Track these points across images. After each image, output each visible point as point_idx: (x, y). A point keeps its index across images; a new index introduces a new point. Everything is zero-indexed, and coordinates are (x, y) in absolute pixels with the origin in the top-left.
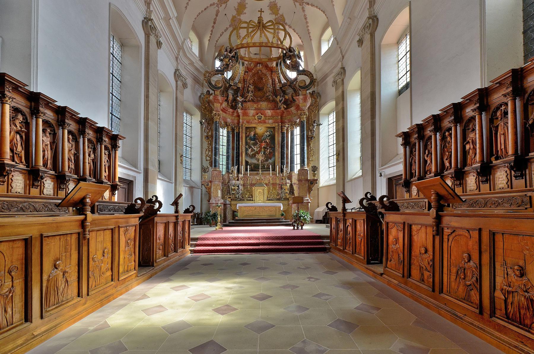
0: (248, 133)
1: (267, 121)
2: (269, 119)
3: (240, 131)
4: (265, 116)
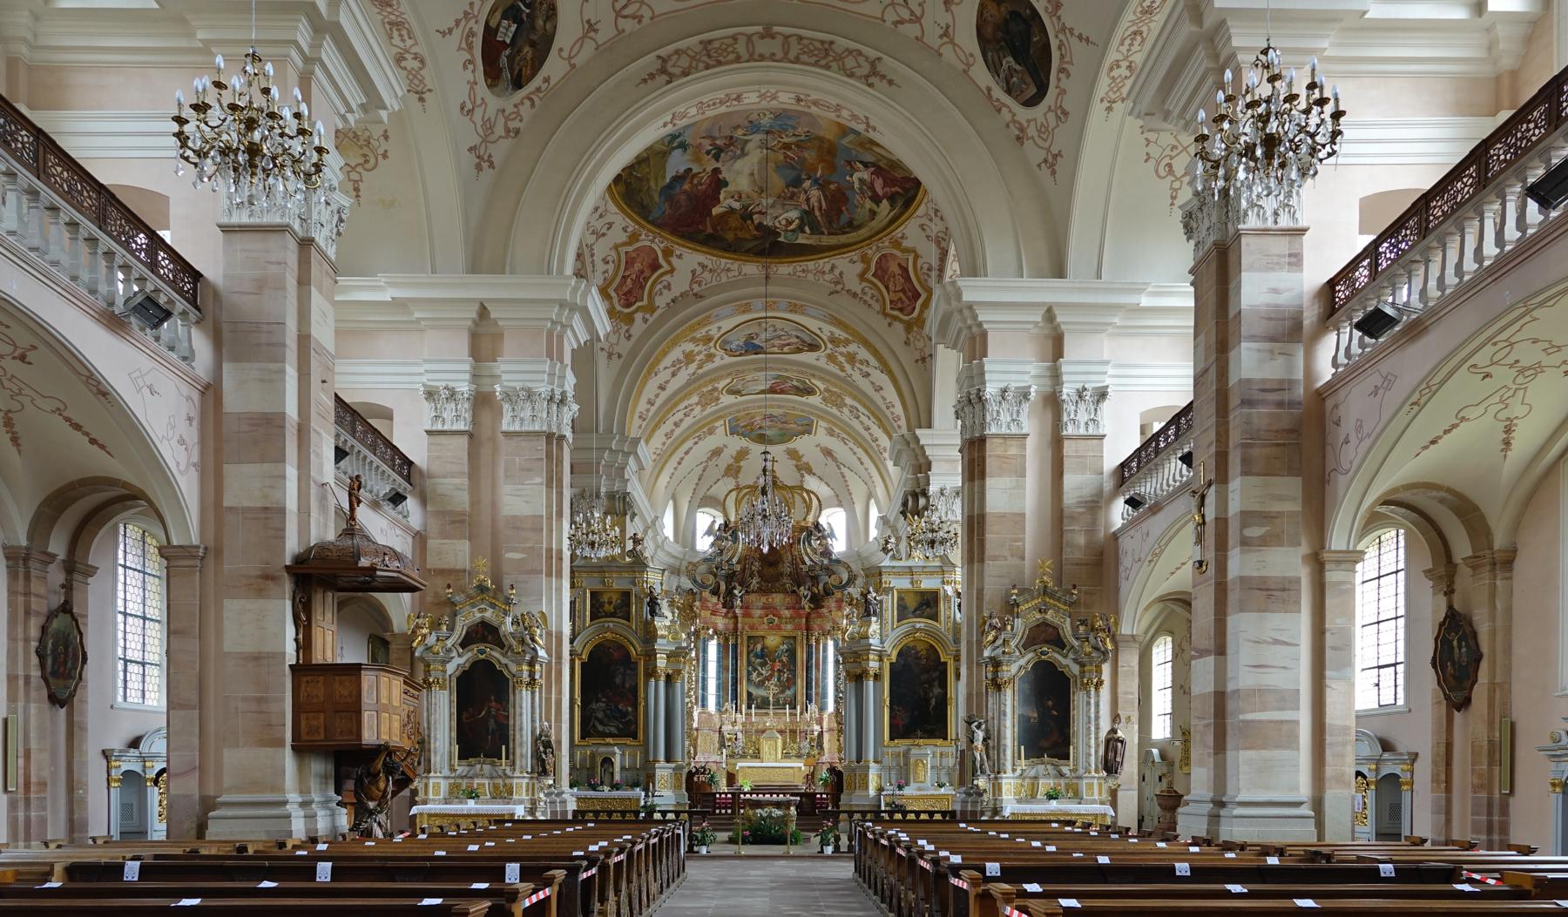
0: (752, 647)
1: (783, 626)
3: (739, 642)
4: (780, 617)
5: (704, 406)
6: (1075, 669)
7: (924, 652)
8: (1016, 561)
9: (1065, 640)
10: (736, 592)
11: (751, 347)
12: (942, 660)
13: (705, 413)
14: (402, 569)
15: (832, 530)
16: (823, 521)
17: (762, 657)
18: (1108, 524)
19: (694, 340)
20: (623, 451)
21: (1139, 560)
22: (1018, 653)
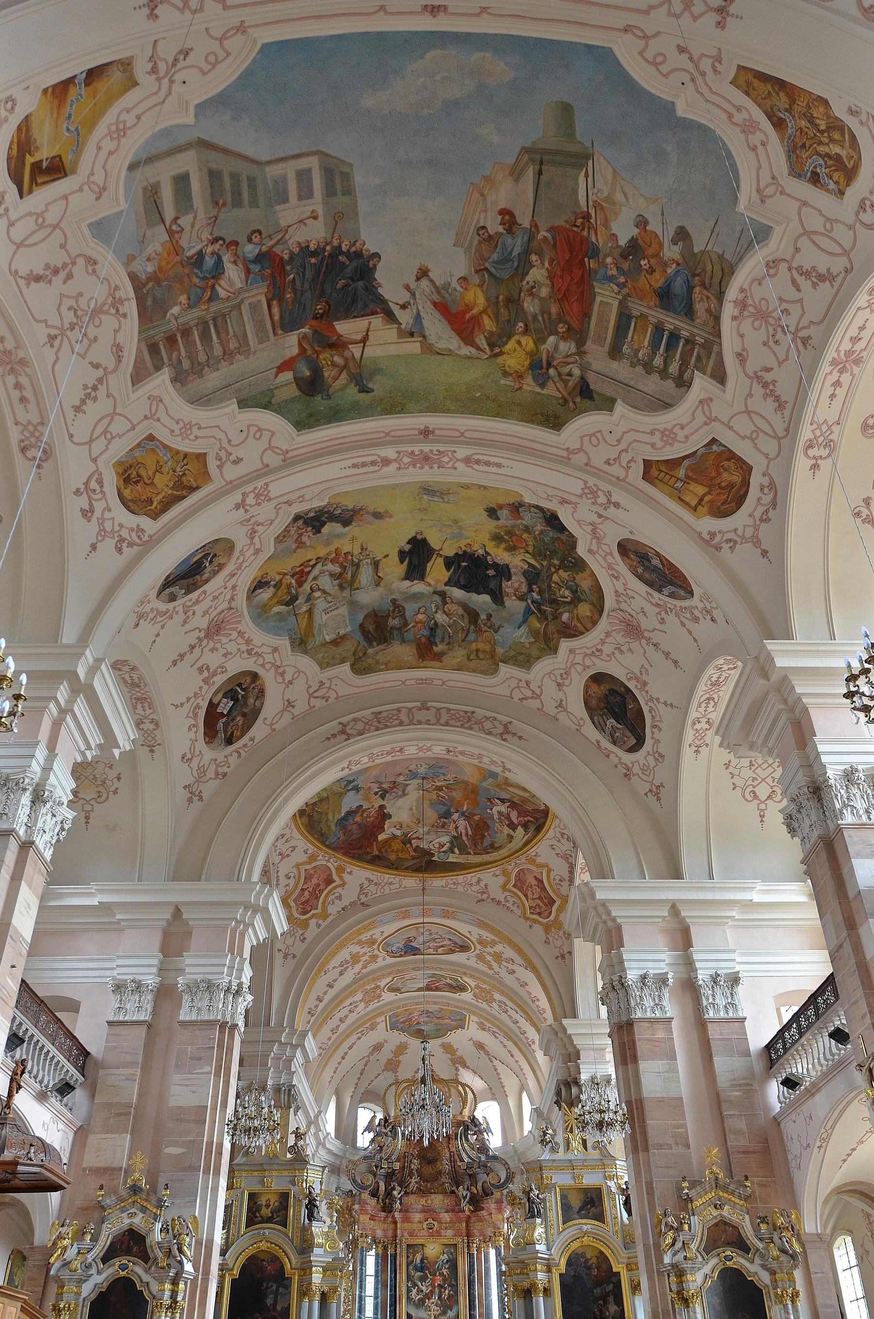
1: (443, 1232)
2: (446, 1228)
3: (398, 1250)
5: (367, 1003)
6: (765, 1278)
7: (594, 1260)
8: (681, 1150)
9: (748, 1242)
10: (395, 1193)
11: (410, 949)
12: (615, 1270)
13: (367, 1010)
14: (46, 1163)
15: (488, 1124)
16: (478, 1115)
17: (422, 1269)
18: (767, 1108)
19: (360, 943)
20: (291, 1044)
21: (808, 1146)
22: (700, 1259)
